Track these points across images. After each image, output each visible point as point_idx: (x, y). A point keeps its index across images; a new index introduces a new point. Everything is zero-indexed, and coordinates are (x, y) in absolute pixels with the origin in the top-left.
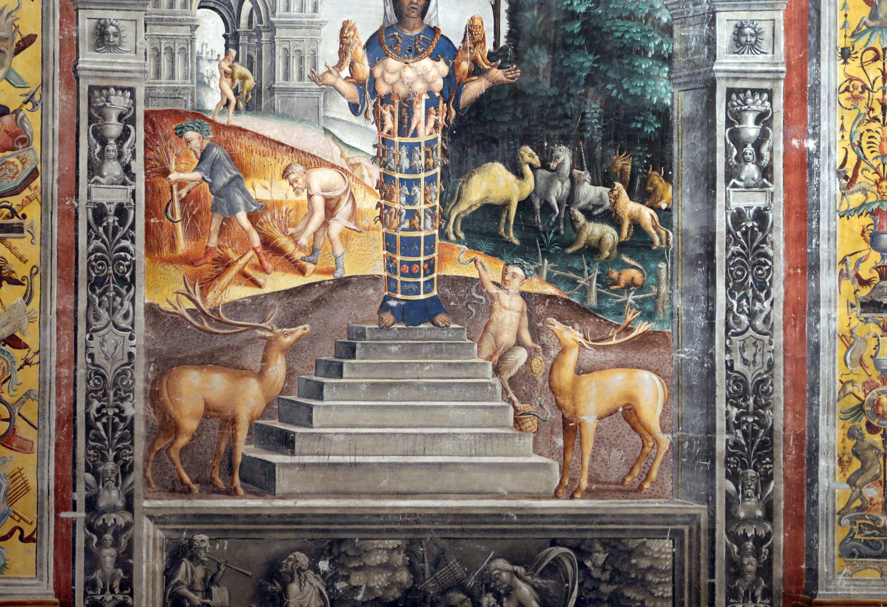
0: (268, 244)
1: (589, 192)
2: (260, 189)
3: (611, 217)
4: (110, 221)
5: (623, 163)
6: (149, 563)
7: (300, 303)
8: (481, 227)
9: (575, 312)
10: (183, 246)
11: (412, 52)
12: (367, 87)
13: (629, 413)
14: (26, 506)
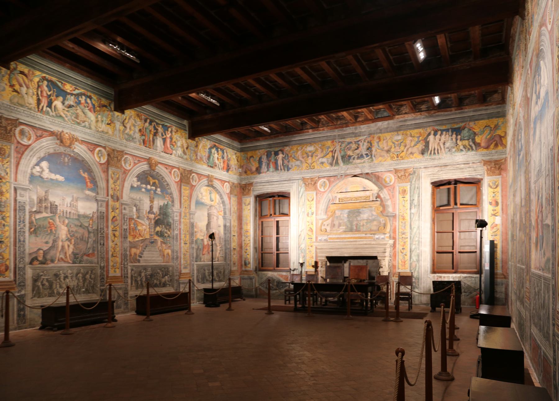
0: (140, 234)
1: (165, 230)
2: (139, 228)
3: (167, 233)
4: (125, 230)
5: (168, 227)
6: (129, 271)
7: (143, 241)
8: (157, 233)
9: (164, 243)
10: (132, 234)
11: (151, 214)
12: (148, 217)
13: (168, 254)
14: (118, 264)
